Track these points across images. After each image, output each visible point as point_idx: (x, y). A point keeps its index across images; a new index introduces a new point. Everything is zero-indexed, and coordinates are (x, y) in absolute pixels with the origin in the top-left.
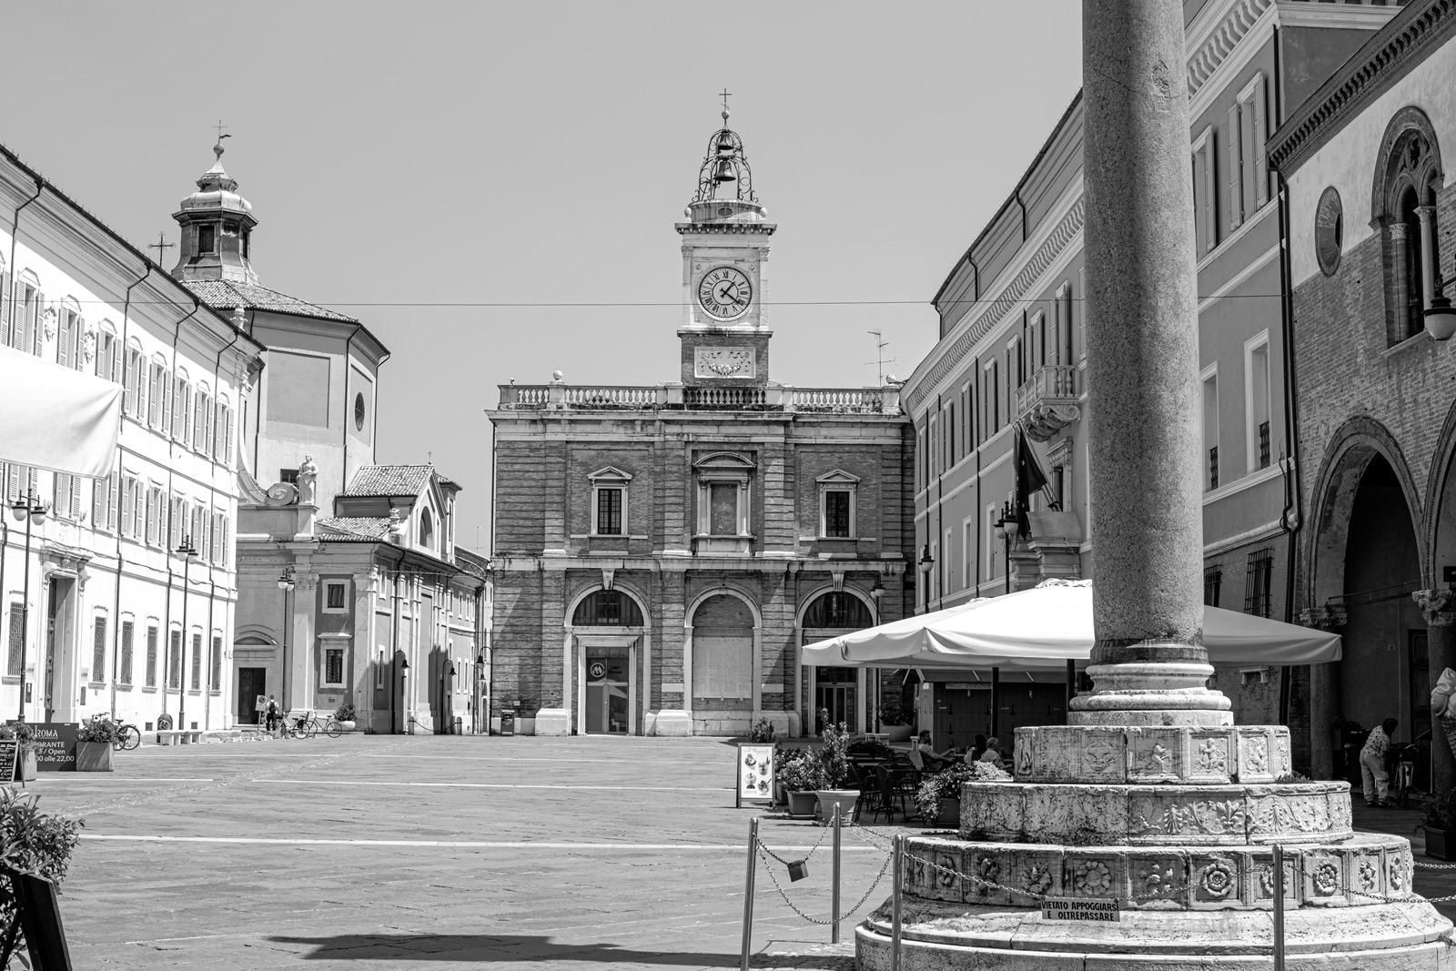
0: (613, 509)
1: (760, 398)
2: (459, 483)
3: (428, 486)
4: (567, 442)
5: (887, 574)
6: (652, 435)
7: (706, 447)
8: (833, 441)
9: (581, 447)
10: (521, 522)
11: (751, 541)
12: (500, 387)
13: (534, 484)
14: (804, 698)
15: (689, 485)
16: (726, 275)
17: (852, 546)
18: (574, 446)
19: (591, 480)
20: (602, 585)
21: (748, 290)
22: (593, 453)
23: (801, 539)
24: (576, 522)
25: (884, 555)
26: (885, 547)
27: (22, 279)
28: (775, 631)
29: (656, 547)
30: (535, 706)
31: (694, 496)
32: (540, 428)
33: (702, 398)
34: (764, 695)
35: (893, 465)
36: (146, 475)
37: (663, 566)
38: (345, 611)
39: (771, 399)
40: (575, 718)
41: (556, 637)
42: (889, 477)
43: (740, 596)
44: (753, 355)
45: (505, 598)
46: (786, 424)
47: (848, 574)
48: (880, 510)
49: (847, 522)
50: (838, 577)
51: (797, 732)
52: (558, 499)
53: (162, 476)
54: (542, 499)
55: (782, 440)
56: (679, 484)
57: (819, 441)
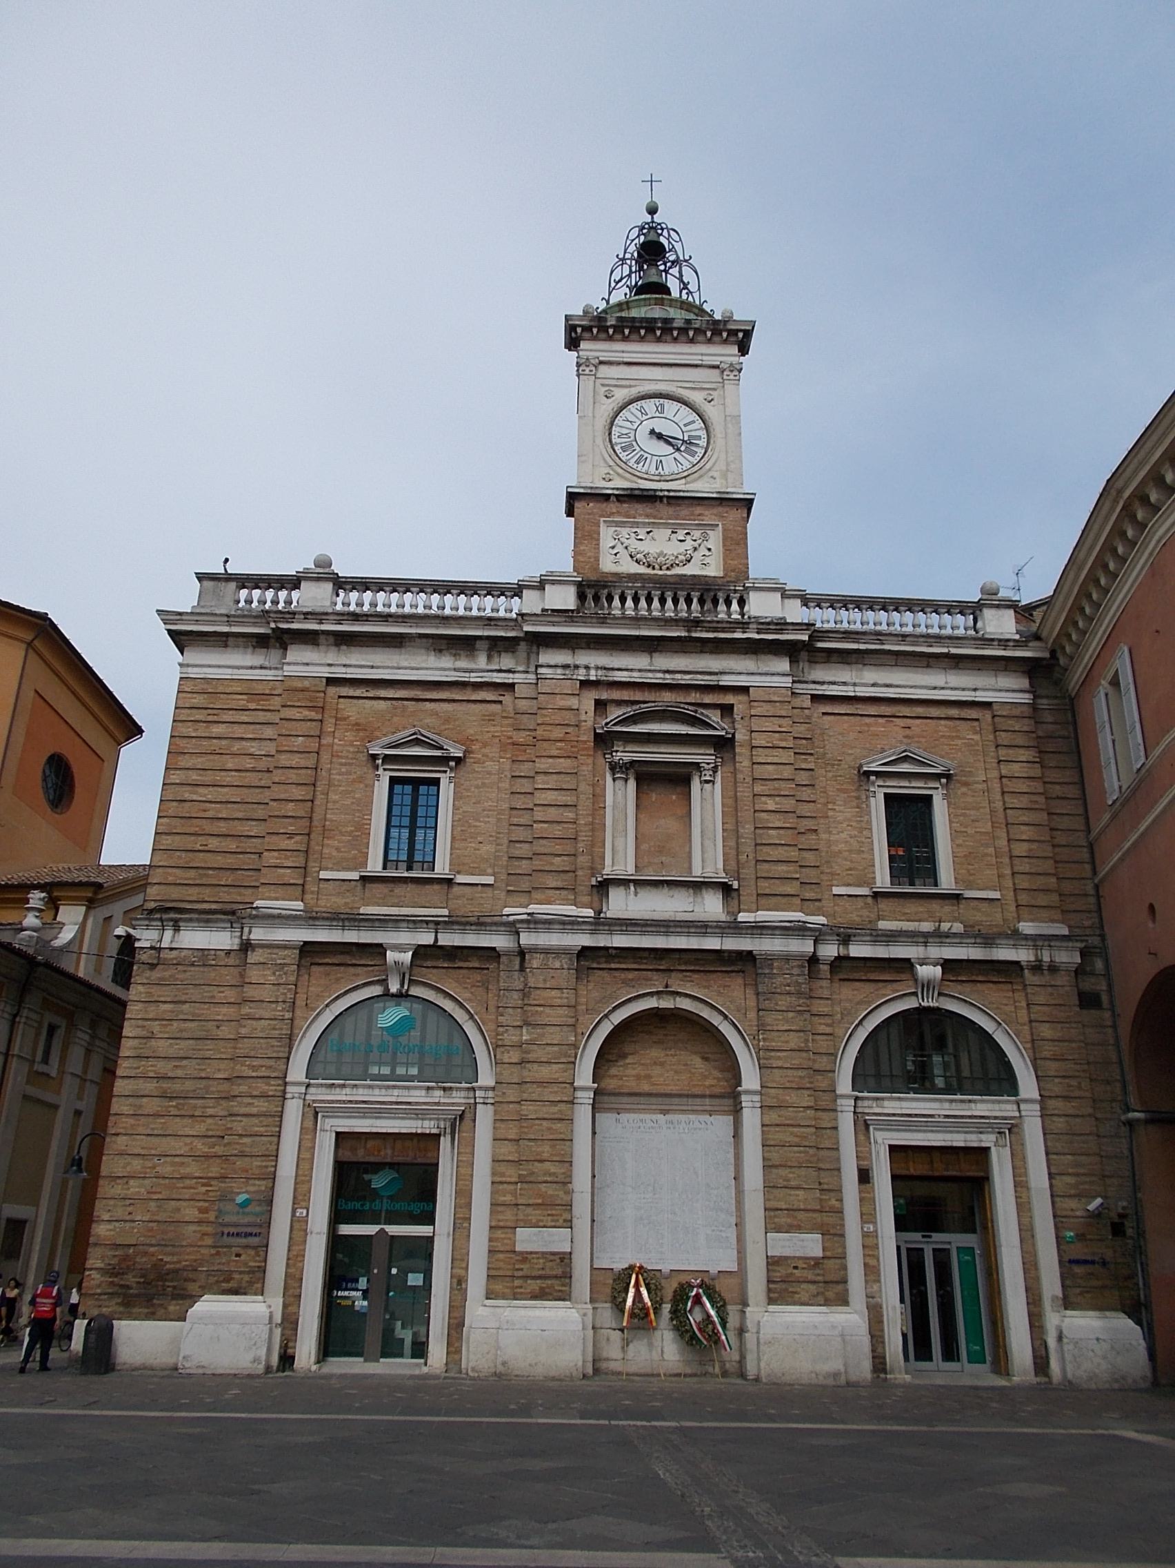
0: (420, 822)
1: (735, 606)
4: (331, 681)
5: (1037, 967)
6: (509, 671)
7: (625, 695)
9: (358, 693)
10: (213, 843)
11: (726, 889)
12: (201, 577)
13: (249, 763)
14: (872, 1272)
15: (586, 770)
17: (947, 908)
18: (345, 691)
19: (374, 757)
20: (383, 982)
21: (703, 434)
22: (382, 705)
23: (836, 890)
24: (332, 847)
25: (1027, 928)
28: (792, 1098)
29: (510, 900)
30: (193, 1288)
31: (598, 797)
32: (274, 656)
33: (616, 602)
34: (773, 1263)
35: (1020, 740)
37: (526, 939)
39: (762, 606)
40: (290, 1322)
41: (261, 1106)
42: (1016, 766)
43: (706, 1013)
44: (715, 539)
45: (152, 1011)
46: (791, 650)
47: (947, 965)
48: (1003, 834)
49: (932, 859)
51: (863, 1369)
52: (298, 793)
54: (266, 796)
56: (564, 764)
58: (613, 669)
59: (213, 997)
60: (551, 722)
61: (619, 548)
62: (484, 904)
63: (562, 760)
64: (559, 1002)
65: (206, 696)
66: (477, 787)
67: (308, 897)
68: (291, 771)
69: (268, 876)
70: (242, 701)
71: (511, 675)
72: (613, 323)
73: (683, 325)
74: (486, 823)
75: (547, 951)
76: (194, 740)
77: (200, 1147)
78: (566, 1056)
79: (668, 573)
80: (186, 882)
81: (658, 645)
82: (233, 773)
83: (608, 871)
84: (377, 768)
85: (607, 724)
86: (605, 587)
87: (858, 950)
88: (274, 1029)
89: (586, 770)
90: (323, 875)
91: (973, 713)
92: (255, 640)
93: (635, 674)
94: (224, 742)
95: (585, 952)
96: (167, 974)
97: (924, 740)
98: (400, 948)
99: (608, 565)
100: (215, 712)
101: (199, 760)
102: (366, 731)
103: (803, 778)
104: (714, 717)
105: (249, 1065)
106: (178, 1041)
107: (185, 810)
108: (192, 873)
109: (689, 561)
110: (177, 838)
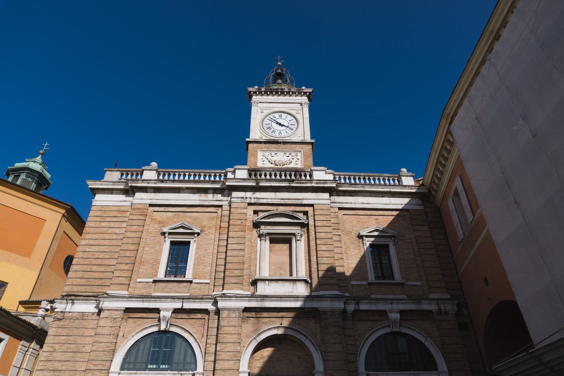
4: (151, 205)
5: (439, 313)
6: (220, 201)
10: (95, 268)
13: (114, 237)
16: (281, 116)
21: (296, 123)
22: (170, 214)
24: (143, 269)
37: (221, 304)
43: (298, 336)
45: (57, 339)
47: (402, 312)
50: (394, 316)
52: (132, 247)
55: (328, 202)
56: (240, 234)
58: (260, 198)
59: (84, 333)
60: (236, 218)
61: (265, 159)
62: (206, 291)
63: (240, 232)
64: (234, 332)
65: (101, 212)
66: (205, 244)
67: (130, 289)
68: (130, 239)
70: (115, 214)
71: (221, 202)
72: (264, 90)
73: (288, 91)
74: (208, 258)
75: (229, 309)
76: (93, 228)
78: (236, 357)
79: (283, 167)
80: (81, 284)
81: (278, 190)
82: (107, 241)
83: (257, 276)
84: (165, 238)
85: (258, 219)
86: (258, 171)
88: (107, 347)
89: (247, 236)
90: (139, 280)
92: (123, 191)
93: (269, 200)
94: (105, 229)
95: (246, 310)
96: (66, 323)
97: (383, 224)
98: (167, 310)
99: (260, 165)
100: (104, 218)
101: (95, 236)
102: (162, 223)
103: (336, 238)
104: (301, 215)
105: (93, 364)
106: (65, 353)
108: (84, 280)
109: (291, 163)
110: (80, 266)
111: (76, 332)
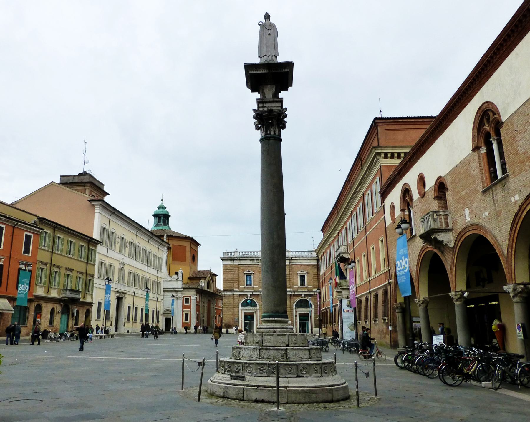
2: (217, 274)
3: (209, 275)
4: (239, 265)
5: (315, 294)
8: (301, 263)
10: (229, 283)
13: (231, 274)
17: (306, 288)
24: (241, 283)
25: (314, 290)
26: (314, 288)
27: (111, 230)
32: (232, 261)
36: (141, 274)
38: (189, 304)
41: (237, 310)
45: (225, 301)
47: (305, 295)
50: (304, 295)
52: (237, 278)
53: (145, 274)
57: (297, 263)
62: (256, 289)
69: (235, 287)
77: (231, 314)
87: (295, 293)
91: (310, 265)
103: (291, 274)
107: (226, 280)
111: (229, 299)
